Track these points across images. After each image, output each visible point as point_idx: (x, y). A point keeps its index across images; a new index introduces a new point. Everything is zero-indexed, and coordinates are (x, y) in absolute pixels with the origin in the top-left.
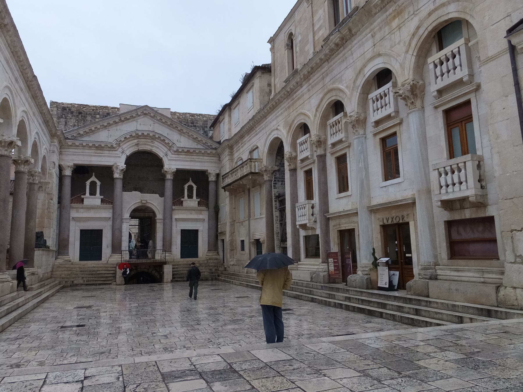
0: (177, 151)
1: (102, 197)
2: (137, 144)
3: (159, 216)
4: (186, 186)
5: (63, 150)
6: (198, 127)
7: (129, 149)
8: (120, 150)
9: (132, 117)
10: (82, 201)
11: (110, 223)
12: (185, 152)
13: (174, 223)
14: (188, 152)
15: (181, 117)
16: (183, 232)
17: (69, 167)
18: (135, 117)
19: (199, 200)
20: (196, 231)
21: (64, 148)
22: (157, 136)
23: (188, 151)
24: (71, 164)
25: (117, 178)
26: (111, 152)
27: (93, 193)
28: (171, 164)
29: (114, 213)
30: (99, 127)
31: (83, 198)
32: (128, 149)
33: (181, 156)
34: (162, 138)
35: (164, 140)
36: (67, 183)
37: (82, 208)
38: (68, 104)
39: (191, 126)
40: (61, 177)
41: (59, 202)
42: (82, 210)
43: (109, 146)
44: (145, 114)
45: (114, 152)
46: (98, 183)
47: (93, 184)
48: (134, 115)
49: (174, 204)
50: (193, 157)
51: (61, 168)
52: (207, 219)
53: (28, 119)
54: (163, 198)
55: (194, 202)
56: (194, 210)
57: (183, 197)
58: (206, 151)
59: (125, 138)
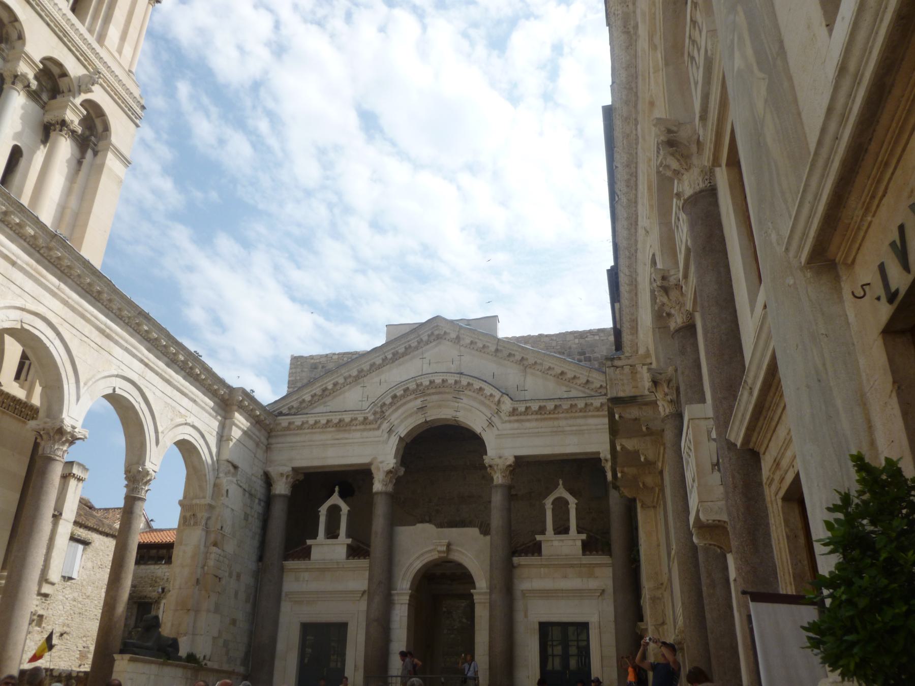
0: (514, 412)
1: (349, 541)
2: (421, 409)
3: (482, 584)
4: (548, 503)
5: (273, 441)
6: (596, 359)
7: (404, 422)
8: (385, 426)
9: (408, 350)
10: (306, 554)
11: (363, 605)
12: (536, 413)
13: (519, 605)
14: (544, 411)
15: (554, 344)
16: (545, 628)
17: (282, 475)
18: (417, 348)
19: (584, 536)
20: (584, 627)
21: (276, 436)
22: (464, 381)
23: (540, 408)
24: (287, 469)
25: (377, 493)
26: (365, 434)
27: (332, 534)
28: (503, 446)
29: (370, 579)
30: (341, 380)
31: (310, 547)
32: (402, 421)
33: (527, 425)
34: (477, 385)
35: (481, 389)
36: (279, 510)
37: (307, 570)
38: (321, 356)
39: (580, 361)
40: (269, 500)
41: (260, 558)
42: (306, 575)
43: (361, 418)
44: (439, 337)
45: (371, 433)
46: (345, 508)
47: (334, 511)
48: (414, 344)
49: (515, 552)
50: (556, 423)
51: (268, 480)
52: (610, 589)
53: (58, 334)
54: (488, 538)
55: (569, 545)
56: (572, 566)
57: (543, 532)
58: (589, 401)
59: (394, 397)
